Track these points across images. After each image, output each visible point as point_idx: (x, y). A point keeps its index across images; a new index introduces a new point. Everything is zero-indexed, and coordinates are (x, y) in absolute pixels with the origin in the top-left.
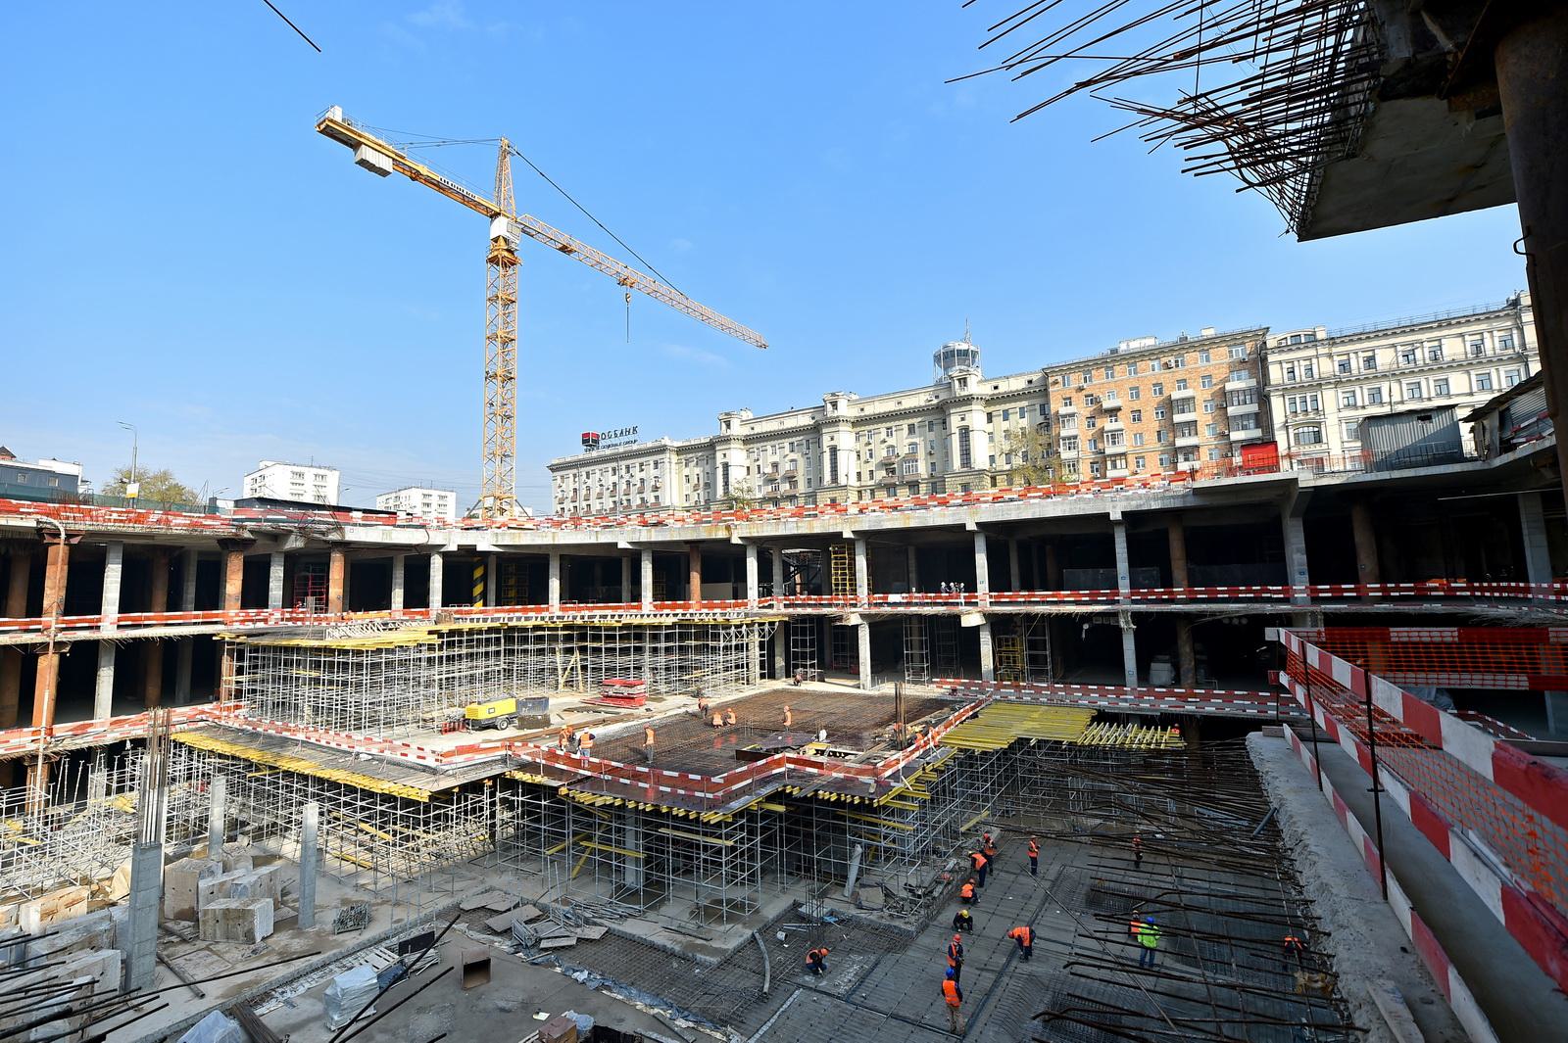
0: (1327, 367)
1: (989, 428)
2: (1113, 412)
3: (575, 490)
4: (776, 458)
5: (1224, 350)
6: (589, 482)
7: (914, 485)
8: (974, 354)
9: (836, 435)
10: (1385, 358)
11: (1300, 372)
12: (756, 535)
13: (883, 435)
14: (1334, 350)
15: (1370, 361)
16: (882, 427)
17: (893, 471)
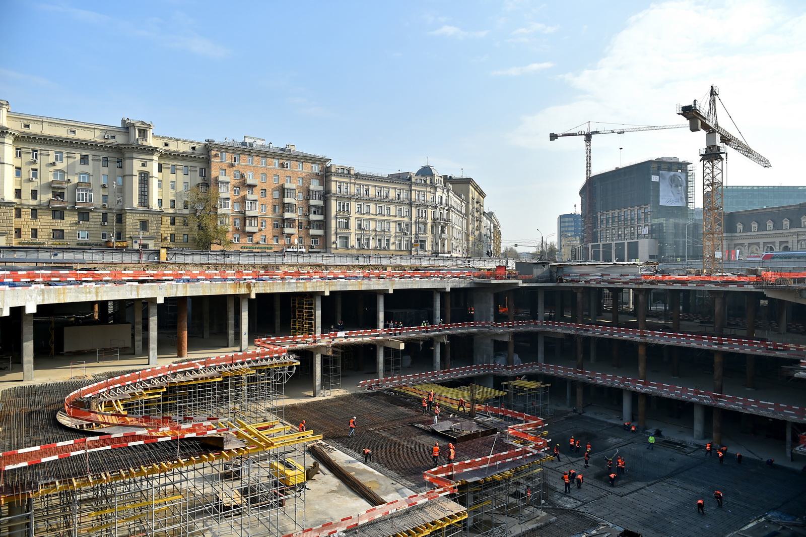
0: (353, 189)
2: (252, 187)
5: (309, 165)
7: (84, 215)
10: (372, 192)
11: (343, 189)
12: (268, 292)
17: (62, 195)
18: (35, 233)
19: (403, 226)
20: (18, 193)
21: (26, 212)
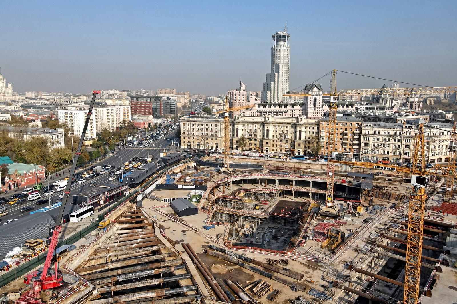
1: (306, 130)
3: (189, 128)
4: (251, 128)
6: (194, 127)
7: (287, 141)
8: (288, 36)
9: (269, 127)
13: (280, 127)
14: (374, 129)
15: (379, 133)
17: (282, 136)
18: (276, 145)
19: (397, 146)
20: (273, 136)
21: (275, 141)
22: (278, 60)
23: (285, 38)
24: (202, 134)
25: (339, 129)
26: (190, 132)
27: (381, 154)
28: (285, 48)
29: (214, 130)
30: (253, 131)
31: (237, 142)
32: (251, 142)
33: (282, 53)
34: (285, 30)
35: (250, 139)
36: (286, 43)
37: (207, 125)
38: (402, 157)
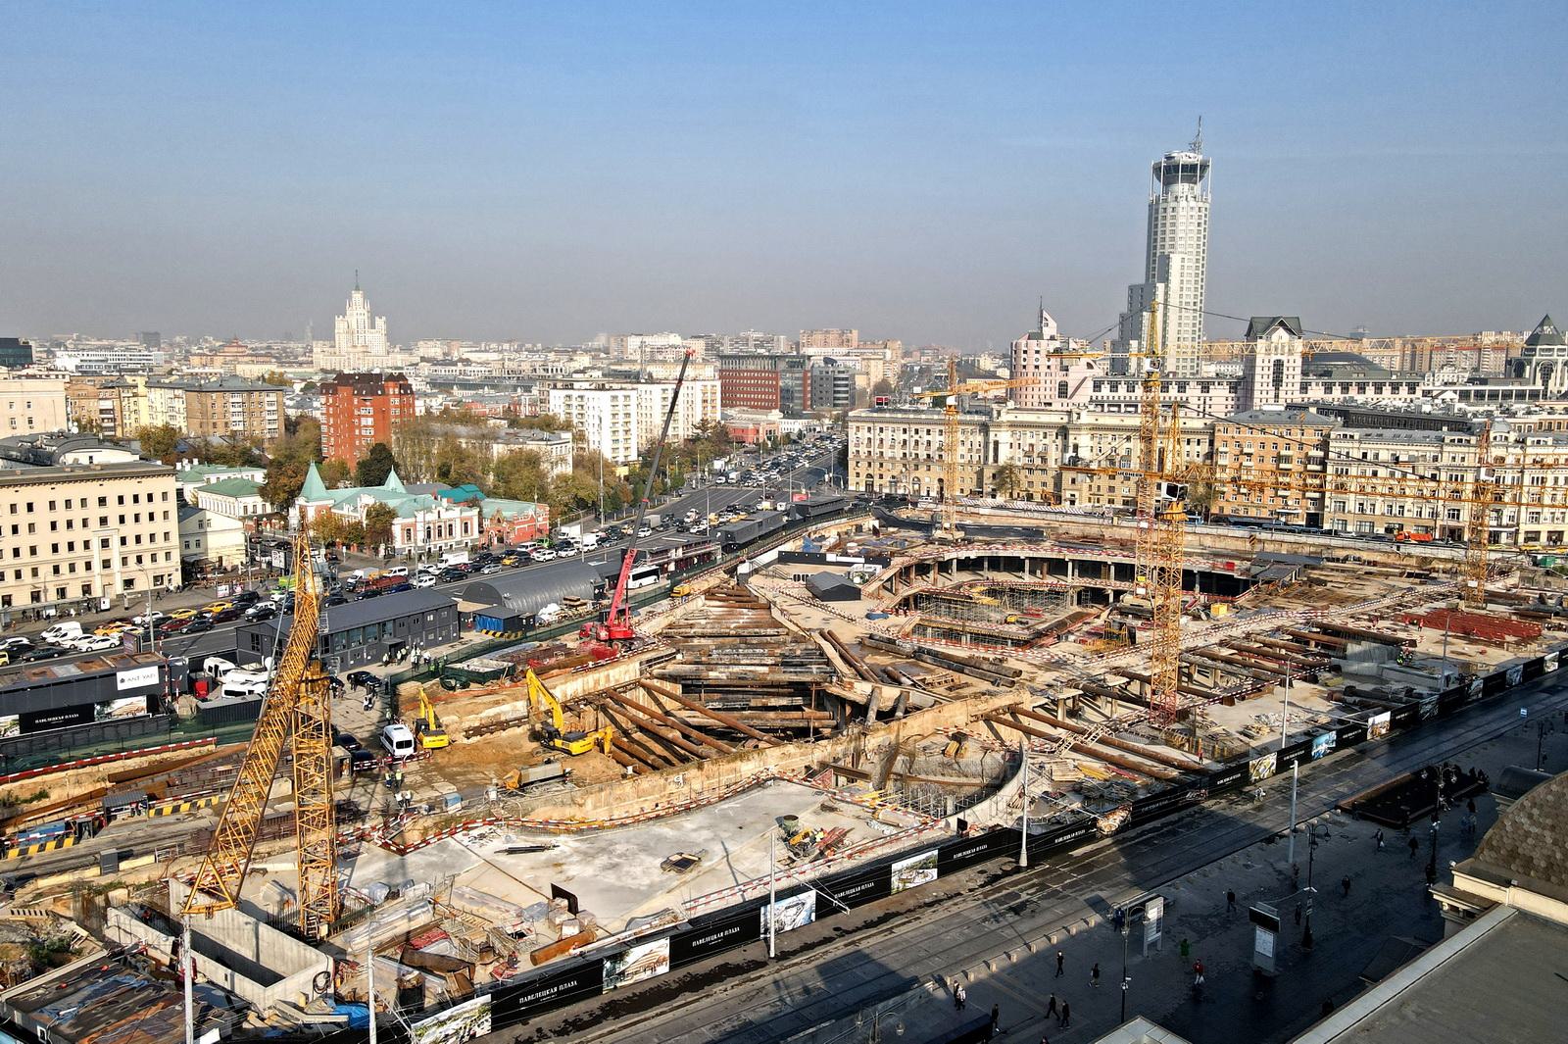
3: (869, 439)
4: (1033, 441)
6: (883, 435)
8: (1204, 167)
13: (1110, 439)
15: (1377, 456)
16: (1110, 434)
22: (1168, 243)
23: (1192, 172)
24: (905, 454)
25: (1269, 446)
26: (872, 450)
27: (1383, 514)
28: (1192, 203)
29: (935, 446)
30: (1039, 448)
31: (994, 476)
32: (1032, 478)
33: (1181, 220)
34: (1195, 147)
35: (1030, 470)
36: (1198, 188)
37: (917, 432)
38: (1439, 523)
